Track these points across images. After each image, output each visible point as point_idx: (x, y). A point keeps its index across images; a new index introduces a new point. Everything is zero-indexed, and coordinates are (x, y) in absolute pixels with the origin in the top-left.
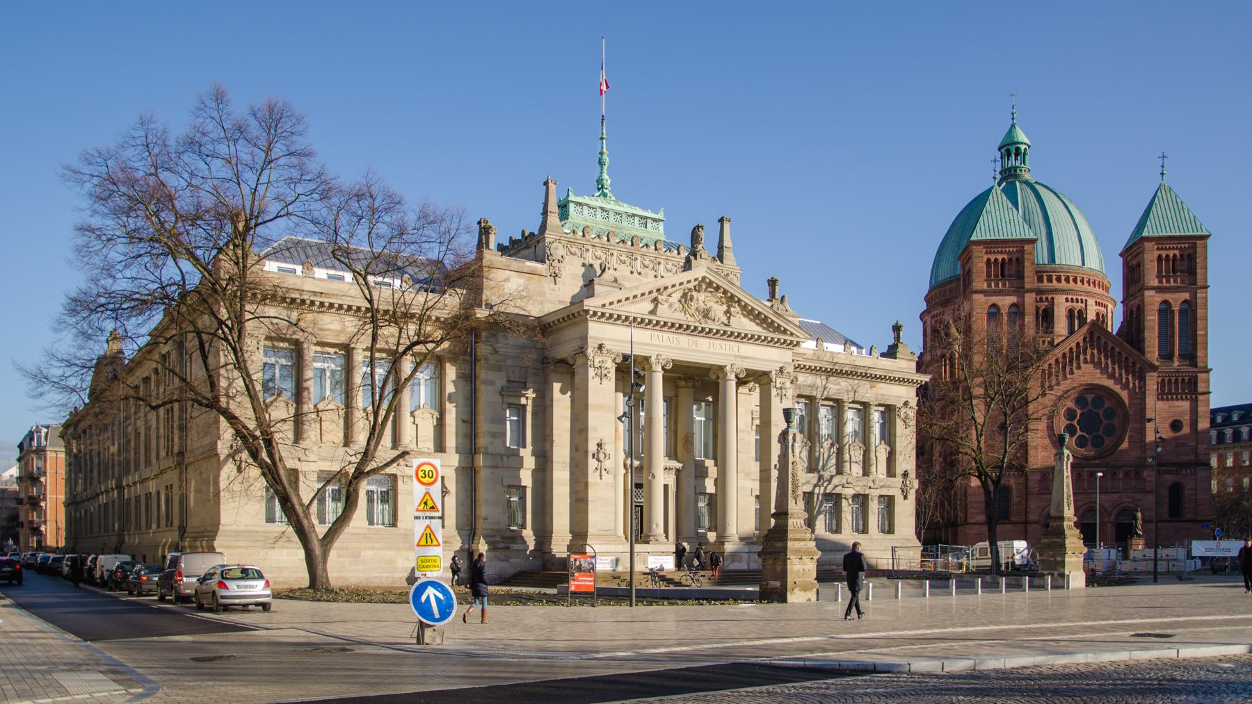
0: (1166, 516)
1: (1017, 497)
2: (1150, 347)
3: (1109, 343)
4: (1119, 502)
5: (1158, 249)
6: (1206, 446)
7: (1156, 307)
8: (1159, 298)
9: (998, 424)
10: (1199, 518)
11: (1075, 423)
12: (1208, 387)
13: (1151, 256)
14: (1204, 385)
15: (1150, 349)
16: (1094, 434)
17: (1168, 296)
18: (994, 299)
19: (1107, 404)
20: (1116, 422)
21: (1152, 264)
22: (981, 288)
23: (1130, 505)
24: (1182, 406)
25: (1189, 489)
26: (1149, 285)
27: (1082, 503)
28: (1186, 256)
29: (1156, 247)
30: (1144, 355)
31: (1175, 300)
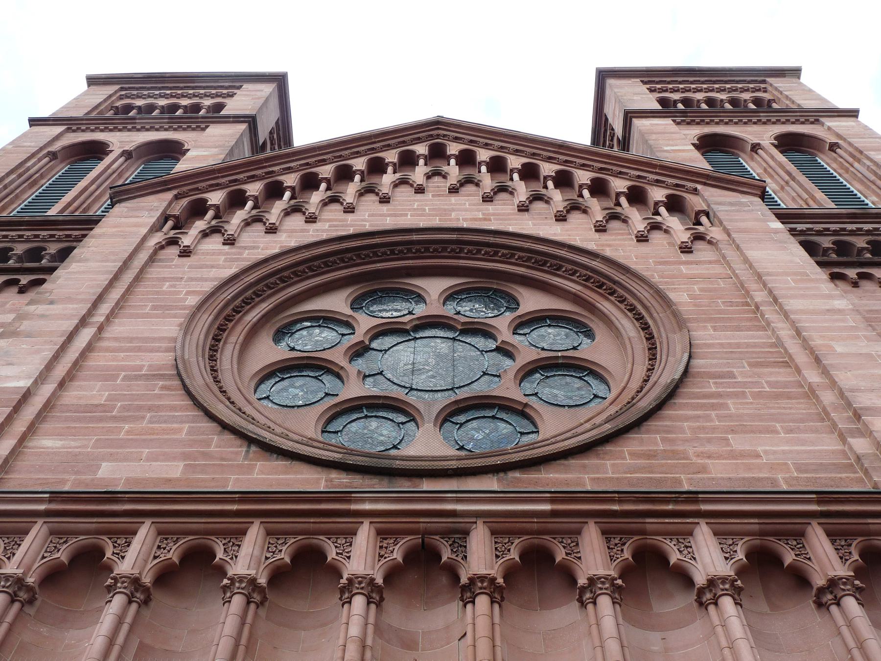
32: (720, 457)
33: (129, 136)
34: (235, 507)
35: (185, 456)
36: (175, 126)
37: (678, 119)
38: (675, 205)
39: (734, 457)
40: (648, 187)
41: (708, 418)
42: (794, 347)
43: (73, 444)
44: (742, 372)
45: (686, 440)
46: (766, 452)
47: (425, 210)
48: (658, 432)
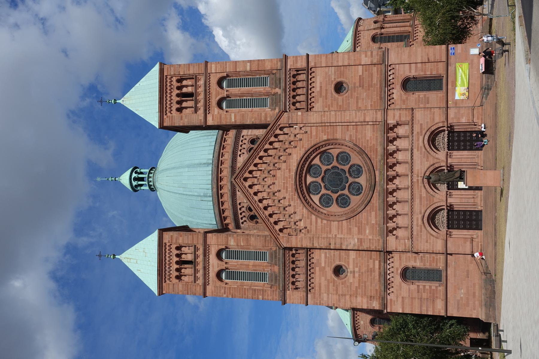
0: (440, 94)
1: (415, 262)
2: (261, 120)
3: (255, 162)
4: (424, 150)
5: (170, 112)
6: (363, 56)
7: (223, 113)
8: (216, 110)
9: (336, 279)
10: (444, 59)
11: (334, 196)
12: (302, 56)
13: (176, 119)
14: (299, 61)
15: (263, 119)
16: (347, 175)
17: (214, 101)
18: (212, 274)
19: (317, 161)
20: (335, 152)
21: (184, 118)
22: (202, 287)
23: (426, 137)
24: (321, 83)
25: (410, 72)
26: (203, 121)
27: (424, 190)
28: (179, 84)
29: (169, 114)
30: (269, 124)
31: (217, 94)
32: (371, 142)
33: (213, 266)
34: (385, 202)
35: (370, 212)
36: (207, 254)
37: (208, 112)
38: (281, 129)
39: (371, 140)
40: (275, 133)
41: (362, 141)
42: (346, 124)
43: (368, 228)
44: (349, 133)
45: (367, 145)
46: (370, 135)
47: (284, 183)
48: (365, 149)
